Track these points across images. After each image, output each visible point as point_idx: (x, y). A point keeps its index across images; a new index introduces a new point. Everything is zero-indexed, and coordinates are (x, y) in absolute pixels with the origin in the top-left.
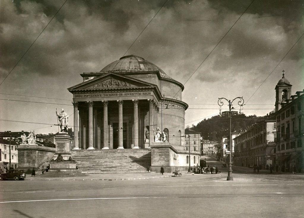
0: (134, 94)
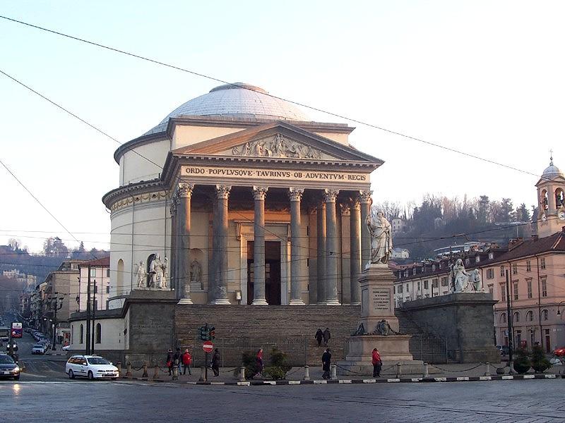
0: (329, 176)
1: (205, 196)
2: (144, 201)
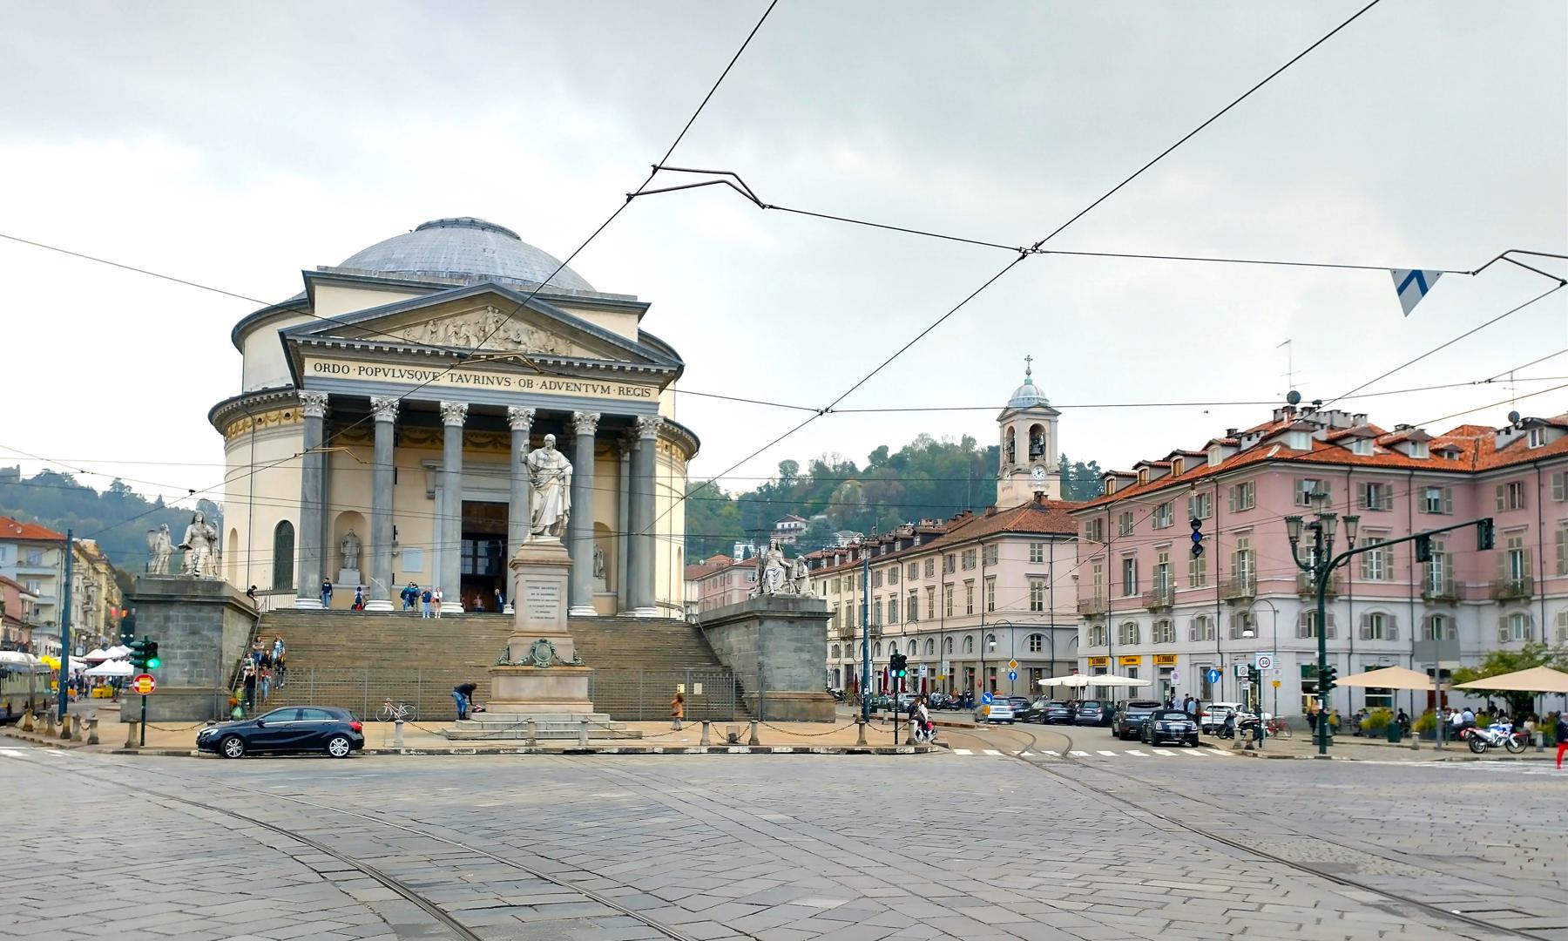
1: (347, 419)
2: (270, 424)
